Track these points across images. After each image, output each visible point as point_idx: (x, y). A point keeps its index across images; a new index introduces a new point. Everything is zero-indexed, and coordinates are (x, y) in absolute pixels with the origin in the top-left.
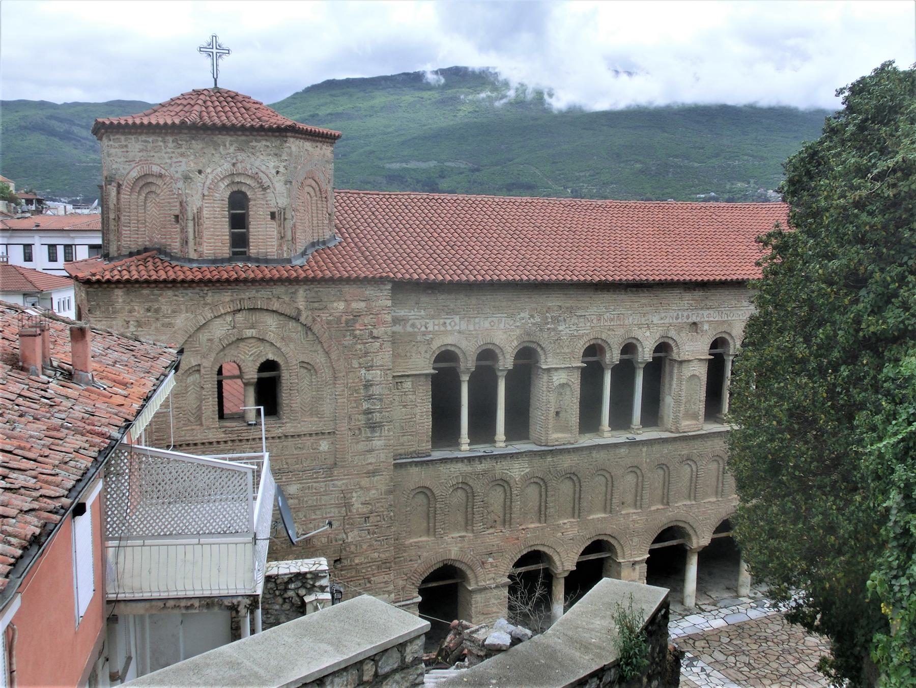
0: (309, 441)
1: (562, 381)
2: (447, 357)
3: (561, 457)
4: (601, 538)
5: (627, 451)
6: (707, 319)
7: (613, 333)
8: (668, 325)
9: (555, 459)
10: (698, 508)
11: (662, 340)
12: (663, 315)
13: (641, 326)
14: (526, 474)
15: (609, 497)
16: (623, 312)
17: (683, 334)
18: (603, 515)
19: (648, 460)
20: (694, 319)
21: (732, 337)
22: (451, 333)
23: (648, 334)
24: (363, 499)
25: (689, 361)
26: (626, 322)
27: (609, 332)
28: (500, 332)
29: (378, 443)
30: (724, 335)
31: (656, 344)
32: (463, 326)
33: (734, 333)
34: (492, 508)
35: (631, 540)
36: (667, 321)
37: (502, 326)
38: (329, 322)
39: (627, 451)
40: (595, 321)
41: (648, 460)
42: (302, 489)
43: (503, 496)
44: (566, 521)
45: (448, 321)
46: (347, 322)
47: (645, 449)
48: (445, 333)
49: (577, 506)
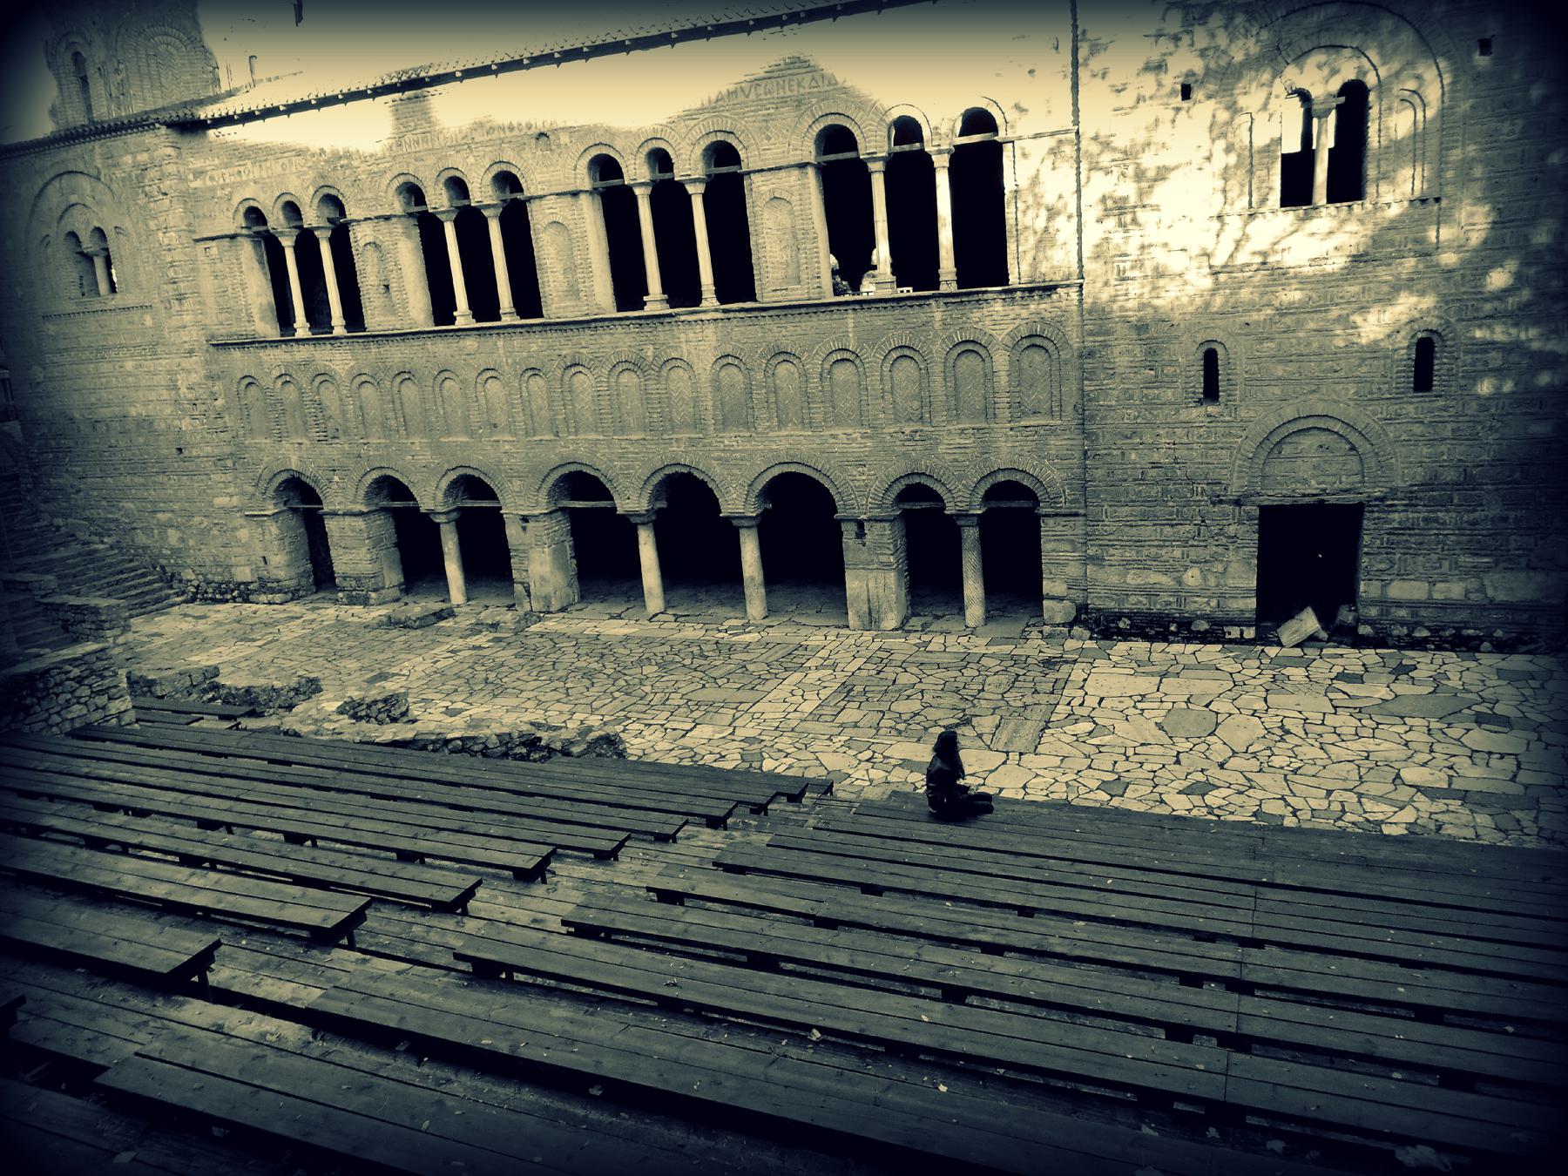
0: (135, 316)
2: (255, 215)
3: (387, 348)
5: (476, 345)
17: (527, 154)
22: (246, 183)
23: (471, 160)
24: (186, 383)
25: (541, 197)
26: (437, 145)
28: (293, 178)
29: (188, 318)
32: (257, 175)
34: (329, 412)
38: (123, 179)
42: (136, 367)
45: (241, 169)
46: (137, 176)
47: (500, 343)
48: (242, 184)
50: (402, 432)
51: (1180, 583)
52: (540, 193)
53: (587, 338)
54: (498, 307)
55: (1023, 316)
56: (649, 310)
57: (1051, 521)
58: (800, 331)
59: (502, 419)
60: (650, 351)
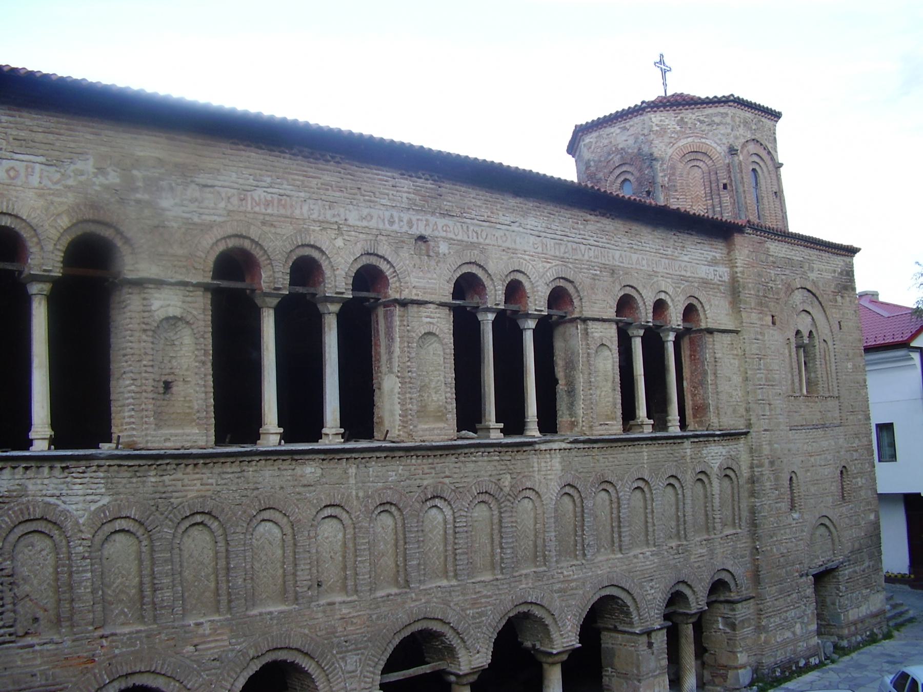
1: (172, 312)
3: (179, 475)
4: (281, 656)
6: (444, 234)
7: (273, 230)
8: (375, 232)
9: (165, 478)
10: (463, 594)
11: (365, 260)
12: (365, 212)
13: (325, 225)
14: (102, 509)
15: (290, 569)
16: (288, 192)
17: (404, 254)
18: (283, 608)
19: (361, 494)
20: (420, 229)
21: (489, 275)
23: (339, 242)
26: (297, 212)
27: (266, 229)
30: (474, 270)
31: (358, 266)
33: (491, 268)
35: (343, 658)
36: (373, 224)
37: (35, 180)
39: (319, 471)
40: (235, 200)
41: (361, 494)
43: (51, 559)
44: (202, 620)
47: (352, 470)
49: (224, 586)
50: (178, 610)
51: (794, 633)
52: (420, 298)
53: (452, 465)
54: (321, 424)
55: (724, 453)
56: (323, 444)
57: (739, 605)
58: (617, 463)
59: (331, 573)
60: (507, 481)
